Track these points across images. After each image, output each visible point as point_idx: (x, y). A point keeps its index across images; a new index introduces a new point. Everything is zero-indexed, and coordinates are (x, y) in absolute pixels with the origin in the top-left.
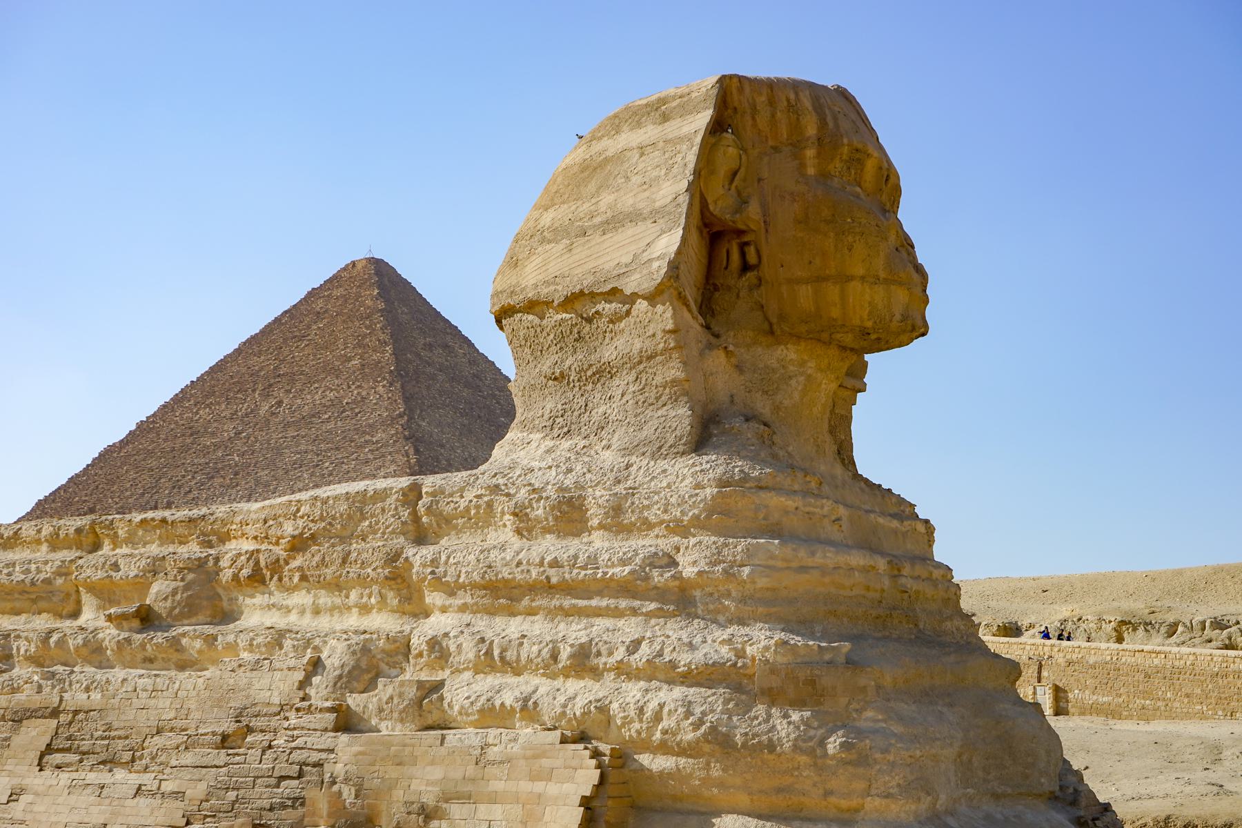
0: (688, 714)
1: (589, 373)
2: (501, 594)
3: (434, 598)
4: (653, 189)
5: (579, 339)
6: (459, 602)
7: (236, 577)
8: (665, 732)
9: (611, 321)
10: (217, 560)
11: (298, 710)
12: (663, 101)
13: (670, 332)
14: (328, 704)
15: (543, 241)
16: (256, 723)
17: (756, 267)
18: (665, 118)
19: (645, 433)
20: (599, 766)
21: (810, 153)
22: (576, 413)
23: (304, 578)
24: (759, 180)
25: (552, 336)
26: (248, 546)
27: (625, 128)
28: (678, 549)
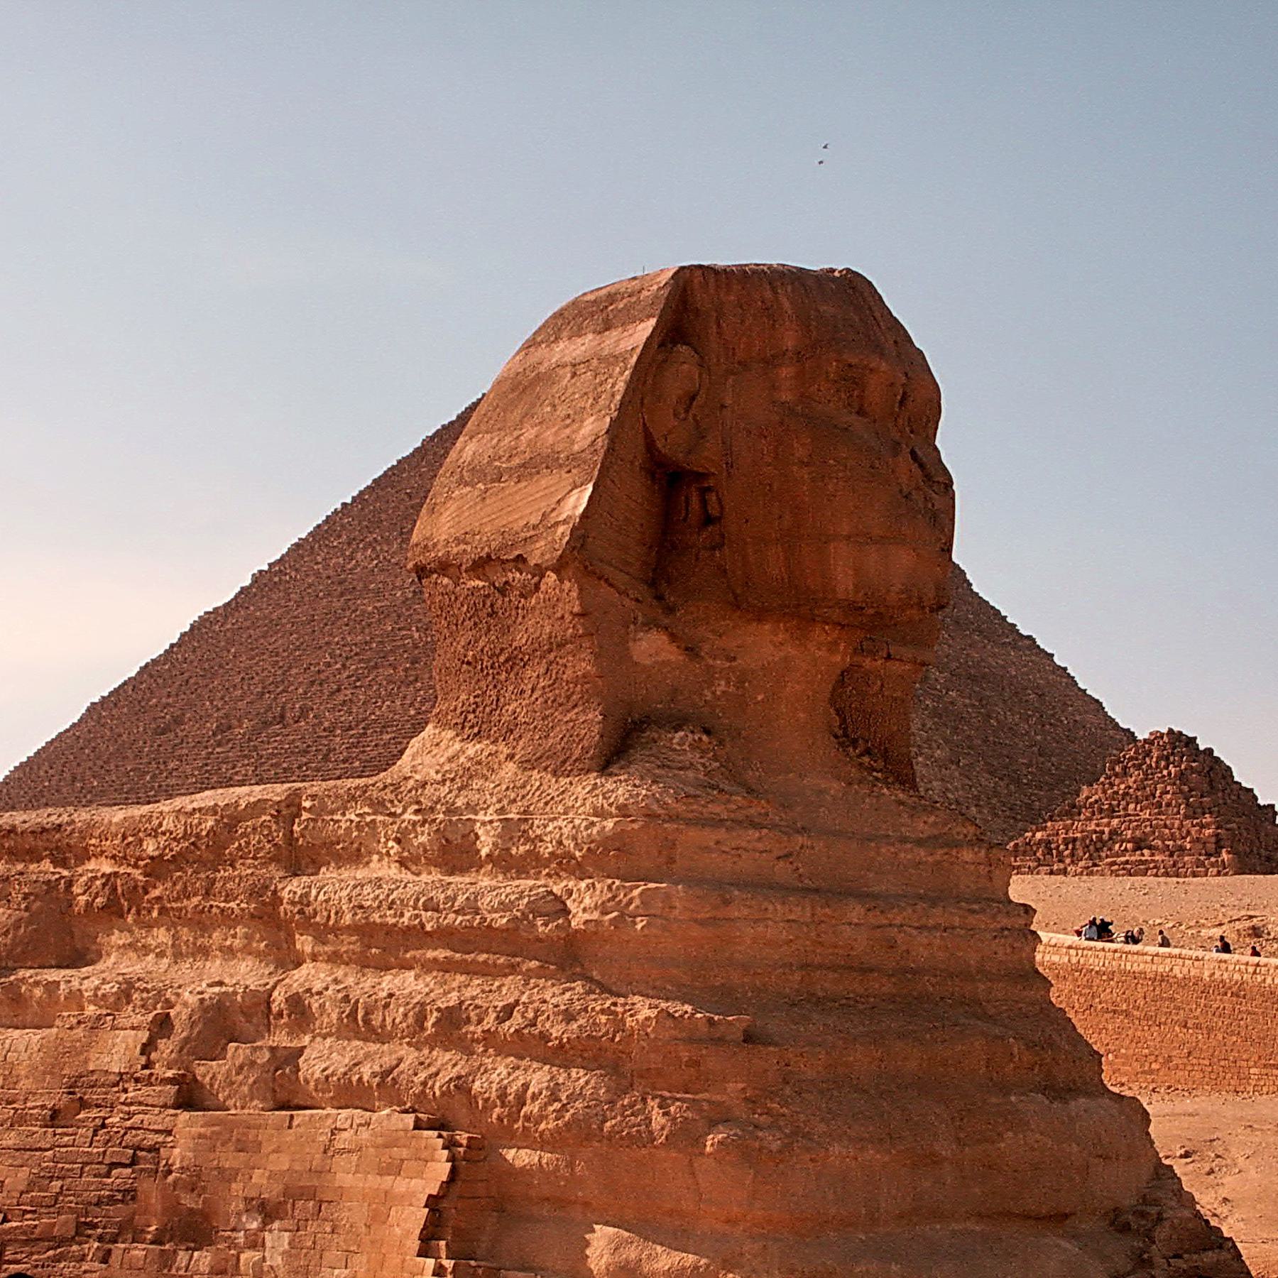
0: (554, 1098)
1: (502, 659)
2: (383, 943)
3: (305, 943)
4: (575, 426)
5: (492, 614)
6: (328, 948)
7: (89, 905)
8: (527, 1118)
9: (522, 595)
10: (70, 884)
11: (137, 1080)
12: (611, 298)
13: (577, 615)
14: (170, 1074)
15: (462, 482)
16: (93, 1096)
17: (719, 519)
18: (608, 326)
19: (551, 741)
20: (452, 1159)
21: (786, 372)
22: (488, 709)
23: (163, 911)
24: (723, 406)
25: (465, 608)
26: (107, 867)
27: (565, 334)
28: (570, 893)
